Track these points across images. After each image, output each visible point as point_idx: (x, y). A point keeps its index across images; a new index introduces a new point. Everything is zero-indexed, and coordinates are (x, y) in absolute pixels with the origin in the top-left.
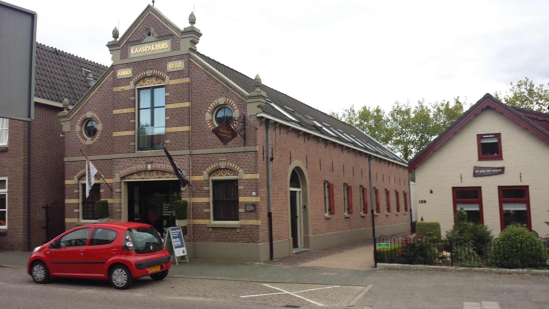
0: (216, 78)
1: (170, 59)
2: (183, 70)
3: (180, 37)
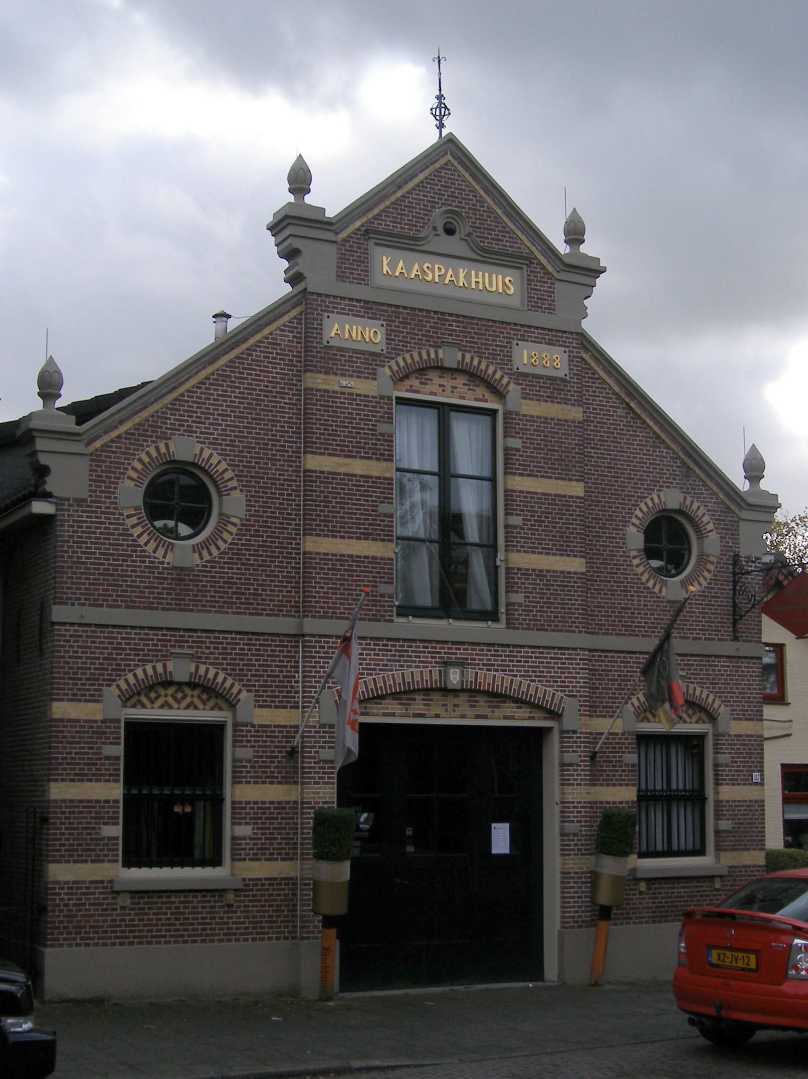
0: (657, 429)
1: (527, 332)
2: (563, 380)
3: (556, 274)
